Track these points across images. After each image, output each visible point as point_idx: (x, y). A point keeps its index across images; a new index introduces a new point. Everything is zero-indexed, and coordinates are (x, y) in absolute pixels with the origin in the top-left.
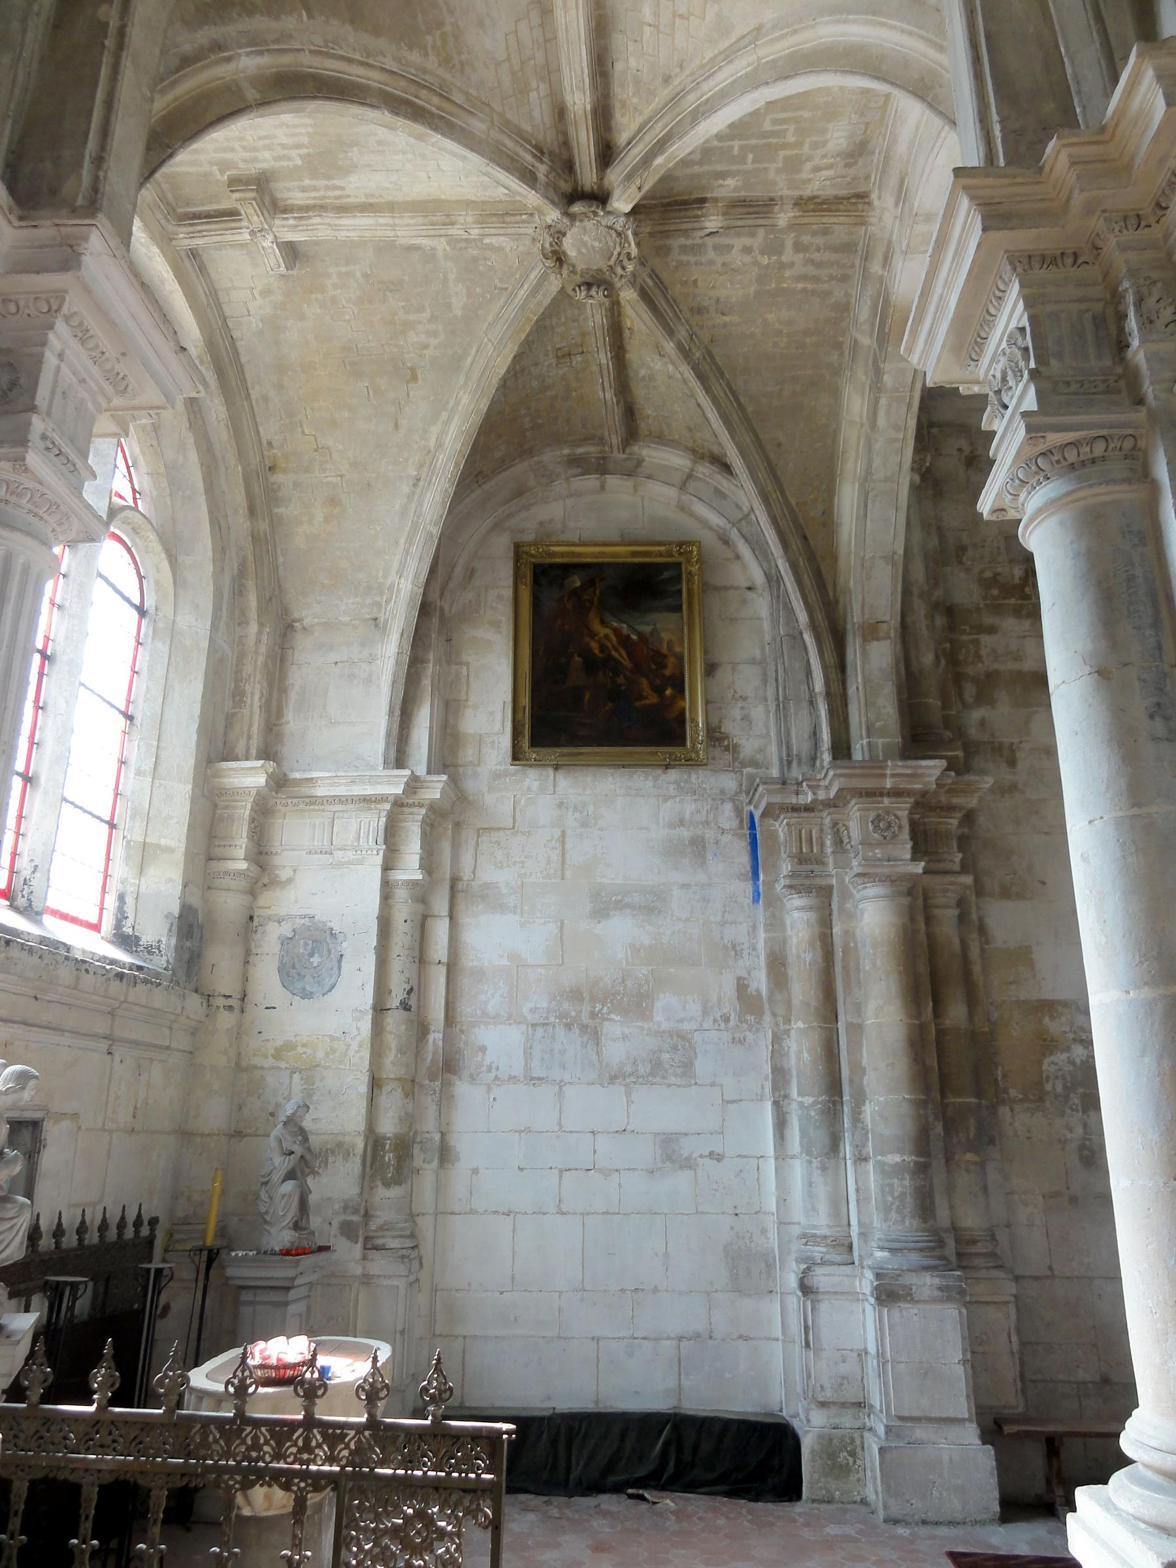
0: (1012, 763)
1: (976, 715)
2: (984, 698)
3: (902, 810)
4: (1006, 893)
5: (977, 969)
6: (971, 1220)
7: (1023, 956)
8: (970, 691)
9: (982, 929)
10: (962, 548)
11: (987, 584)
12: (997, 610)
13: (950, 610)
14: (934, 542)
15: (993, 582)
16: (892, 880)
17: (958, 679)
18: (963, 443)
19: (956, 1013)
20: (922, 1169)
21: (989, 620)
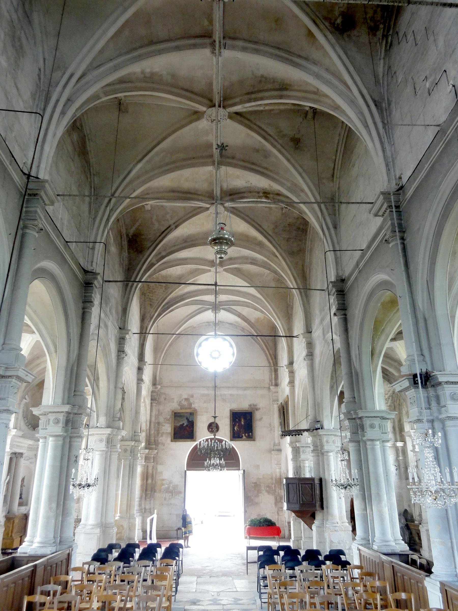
0: (164, 446)
1: (160, 438)
2: (162, 436)
3: (144, 456)
4: (160, 464)
5: (154, 475)
6: (147, 507)
7: (161, 473)
8: (160, 435)
9: (157, 469)
10: (162, 413)
11: (165, 419)
12: (165, 423)
13: (159, 423)
14: (157, 413)
15: (165, 419)
16: (141, 465)
17: (158, 434)
18: (164, 396)
19: (150, 481)
20: (140, 501)
21: (164, 424)
